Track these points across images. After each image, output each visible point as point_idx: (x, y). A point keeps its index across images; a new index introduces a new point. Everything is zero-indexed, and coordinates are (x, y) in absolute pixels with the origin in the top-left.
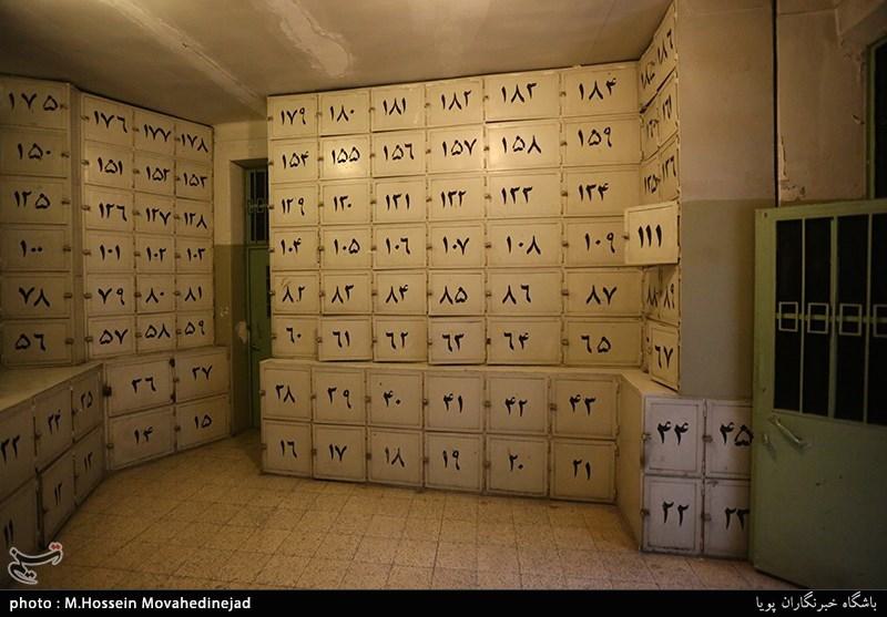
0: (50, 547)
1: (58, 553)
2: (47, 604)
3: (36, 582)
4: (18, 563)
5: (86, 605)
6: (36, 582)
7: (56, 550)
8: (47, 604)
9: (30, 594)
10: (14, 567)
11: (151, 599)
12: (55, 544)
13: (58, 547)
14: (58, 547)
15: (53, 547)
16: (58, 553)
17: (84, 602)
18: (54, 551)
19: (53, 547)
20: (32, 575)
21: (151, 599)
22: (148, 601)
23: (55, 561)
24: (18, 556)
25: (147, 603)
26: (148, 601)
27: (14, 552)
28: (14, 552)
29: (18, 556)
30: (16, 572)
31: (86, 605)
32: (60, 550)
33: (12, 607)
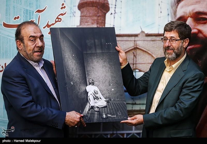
0: (11, 128)
1: (13, 129)
2: (10, 141)
3: (8, 136)
4: (5, 132)
5: (15, 141)
6: (8, 136)
7: (13, 128)
8: (10, 141)
9: (6, 138)
10: (3, 132)
11: (28, 140)
12: (13, 127)
13: (13, 128)
14: (13, 128)
15: (12, 128)
16: (13, 129)
17: (14, 141)
18: (12, 129)
19: (12, 128)
20: (7, 134)
21: (28, 140)
22: (27, 140)
23: (13, 131)
24: (4, 130)
25: (27, 141)
26: (27, 140)
27: (3, 129)
28: (3, 129)
29: (4, 130)
30: (3, 133)
31: (15, 141)
32: (14, 128)
33: (3, 142)
